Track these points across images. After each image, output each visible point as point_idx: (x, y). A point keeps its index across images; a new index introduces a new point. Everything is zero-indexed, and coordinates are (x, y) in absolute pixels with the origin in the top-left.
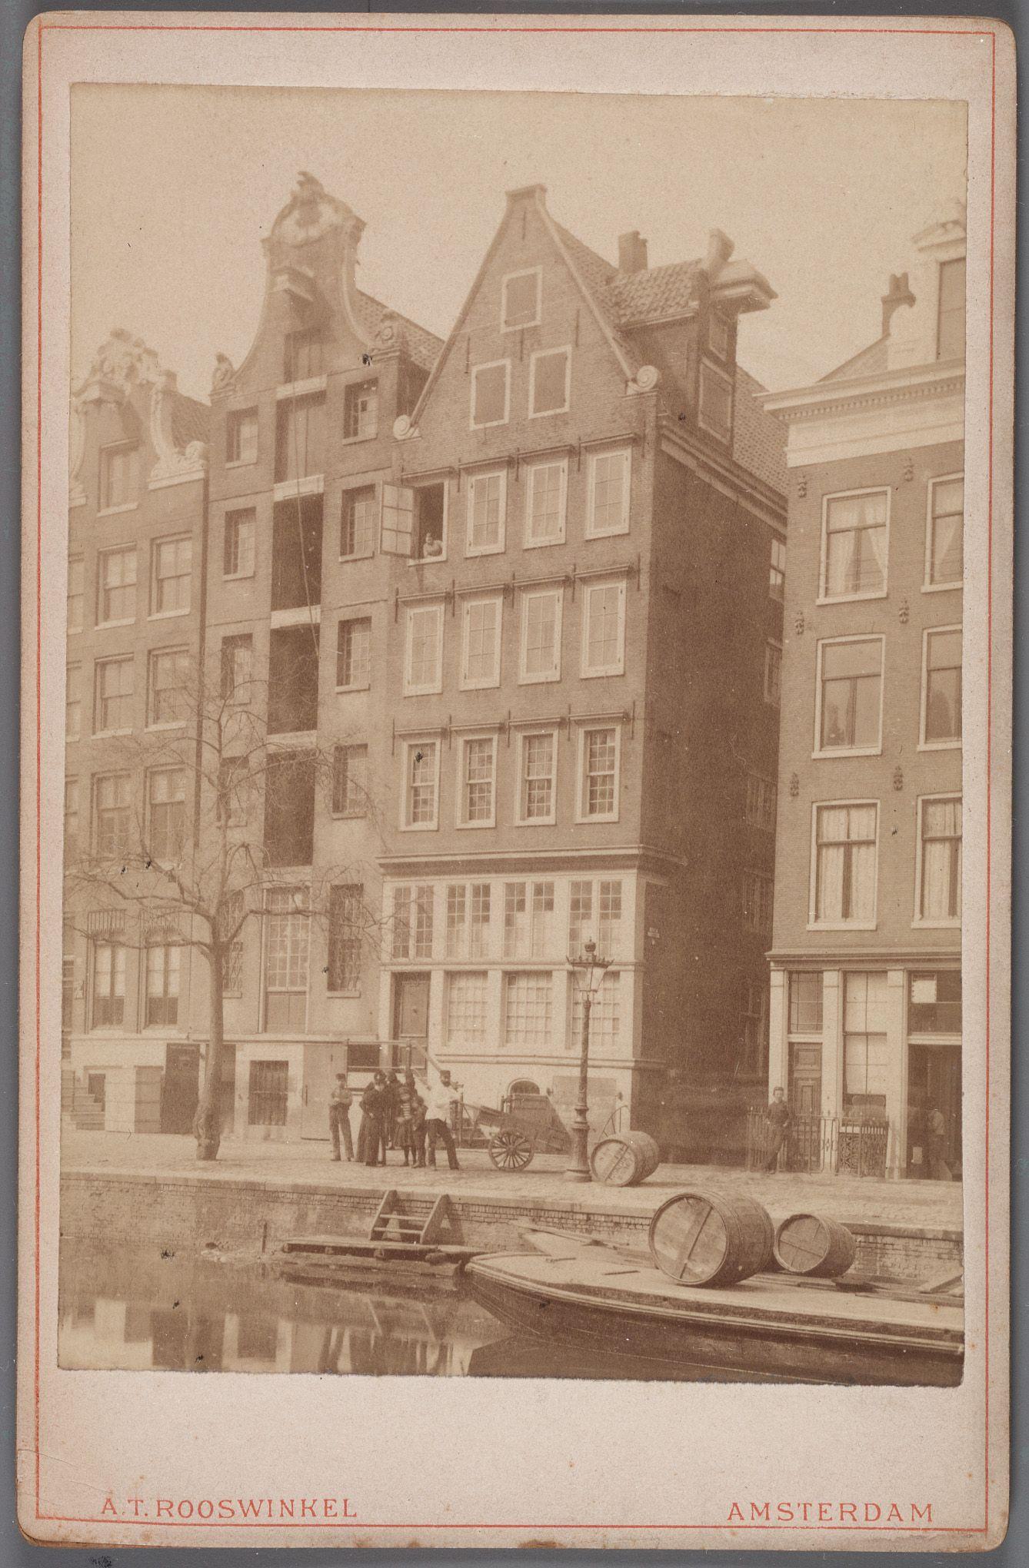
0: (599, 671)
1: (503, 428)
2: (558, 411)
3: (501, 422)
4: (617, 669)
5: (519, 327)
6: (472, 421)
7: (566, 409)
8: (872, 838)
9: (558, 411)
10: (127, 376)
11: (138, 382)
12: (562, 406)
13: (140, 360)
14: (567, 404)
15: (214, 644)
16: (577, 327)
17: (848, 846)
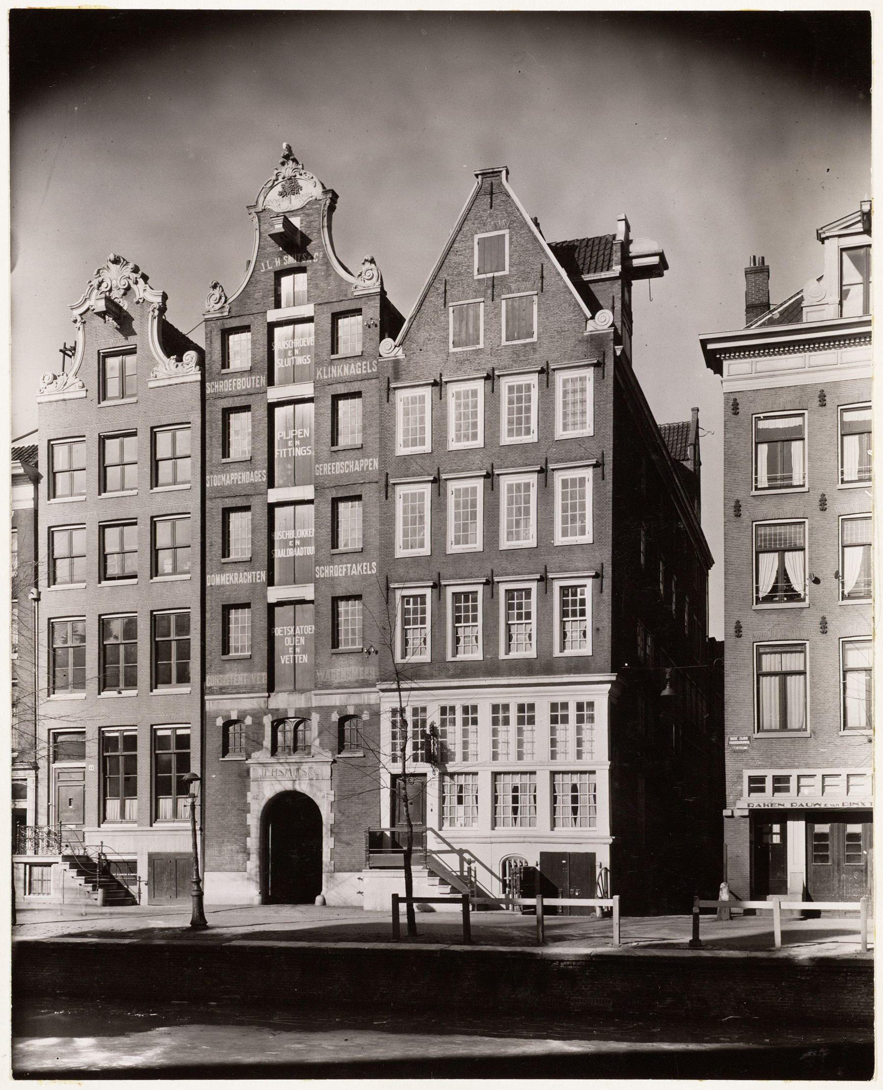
0: (570, 540)
1: (477, 352)
2: (528, 340)
3: (478, 347)
4: (588, 538)
5: (490, 275)
6: (451, 345)
7: (535, 339)
8: (802, 669)
9: (528, 340)
10: (125, 294)
11: (135, 300)
12: (531, 335)
13: (136, 283)
14: (535, 335)
15: (215, 508)
16: (542, 277)
17: (784, 675)
